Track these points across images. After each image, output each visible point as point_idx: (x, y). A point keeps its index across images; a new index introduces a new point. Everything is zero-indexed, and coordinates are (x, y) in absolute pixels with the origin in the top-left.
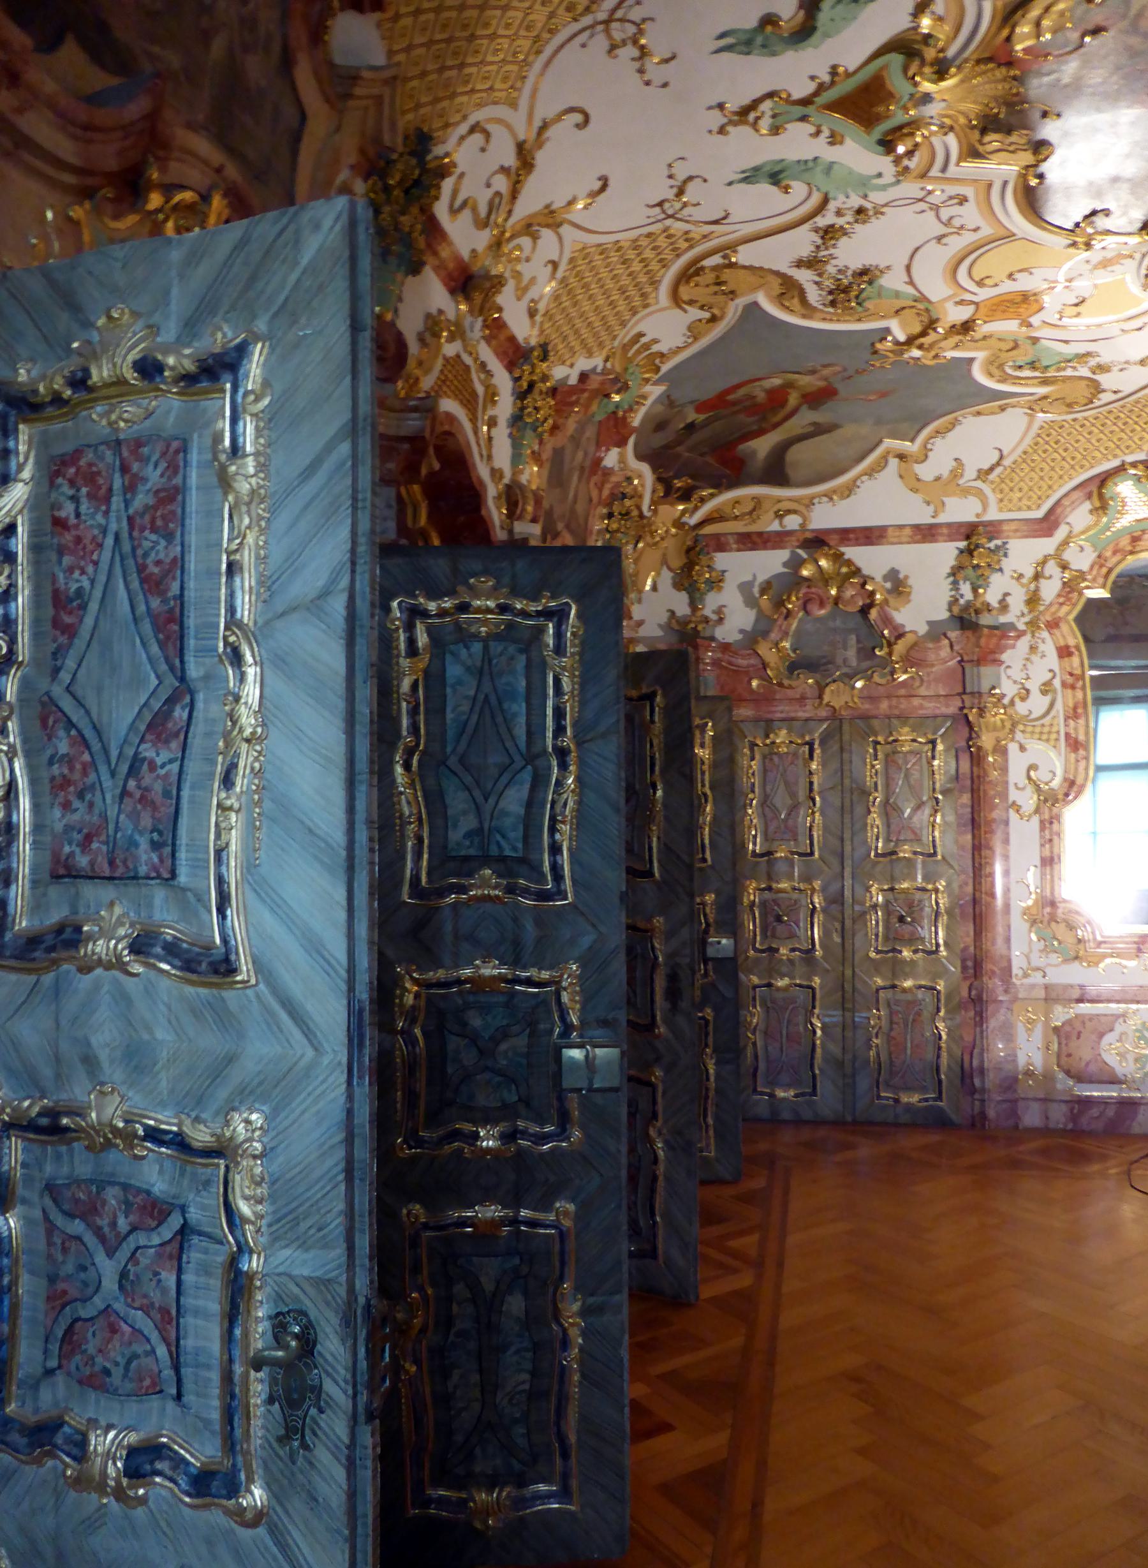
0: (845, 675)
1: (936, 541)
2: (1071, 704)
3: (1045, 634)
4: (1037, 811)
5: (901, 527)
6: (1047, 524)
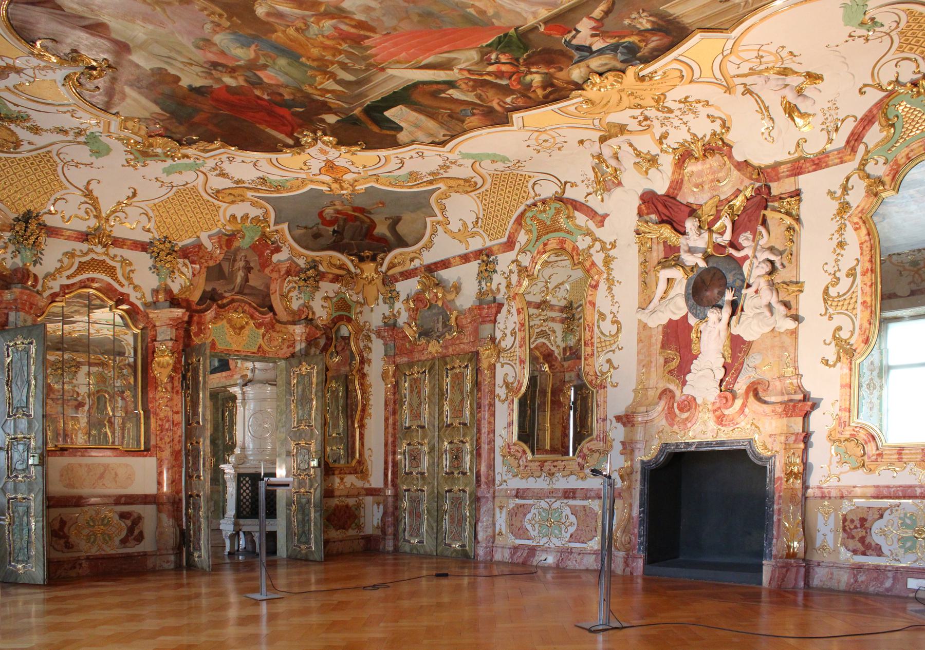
5: (454, 257)
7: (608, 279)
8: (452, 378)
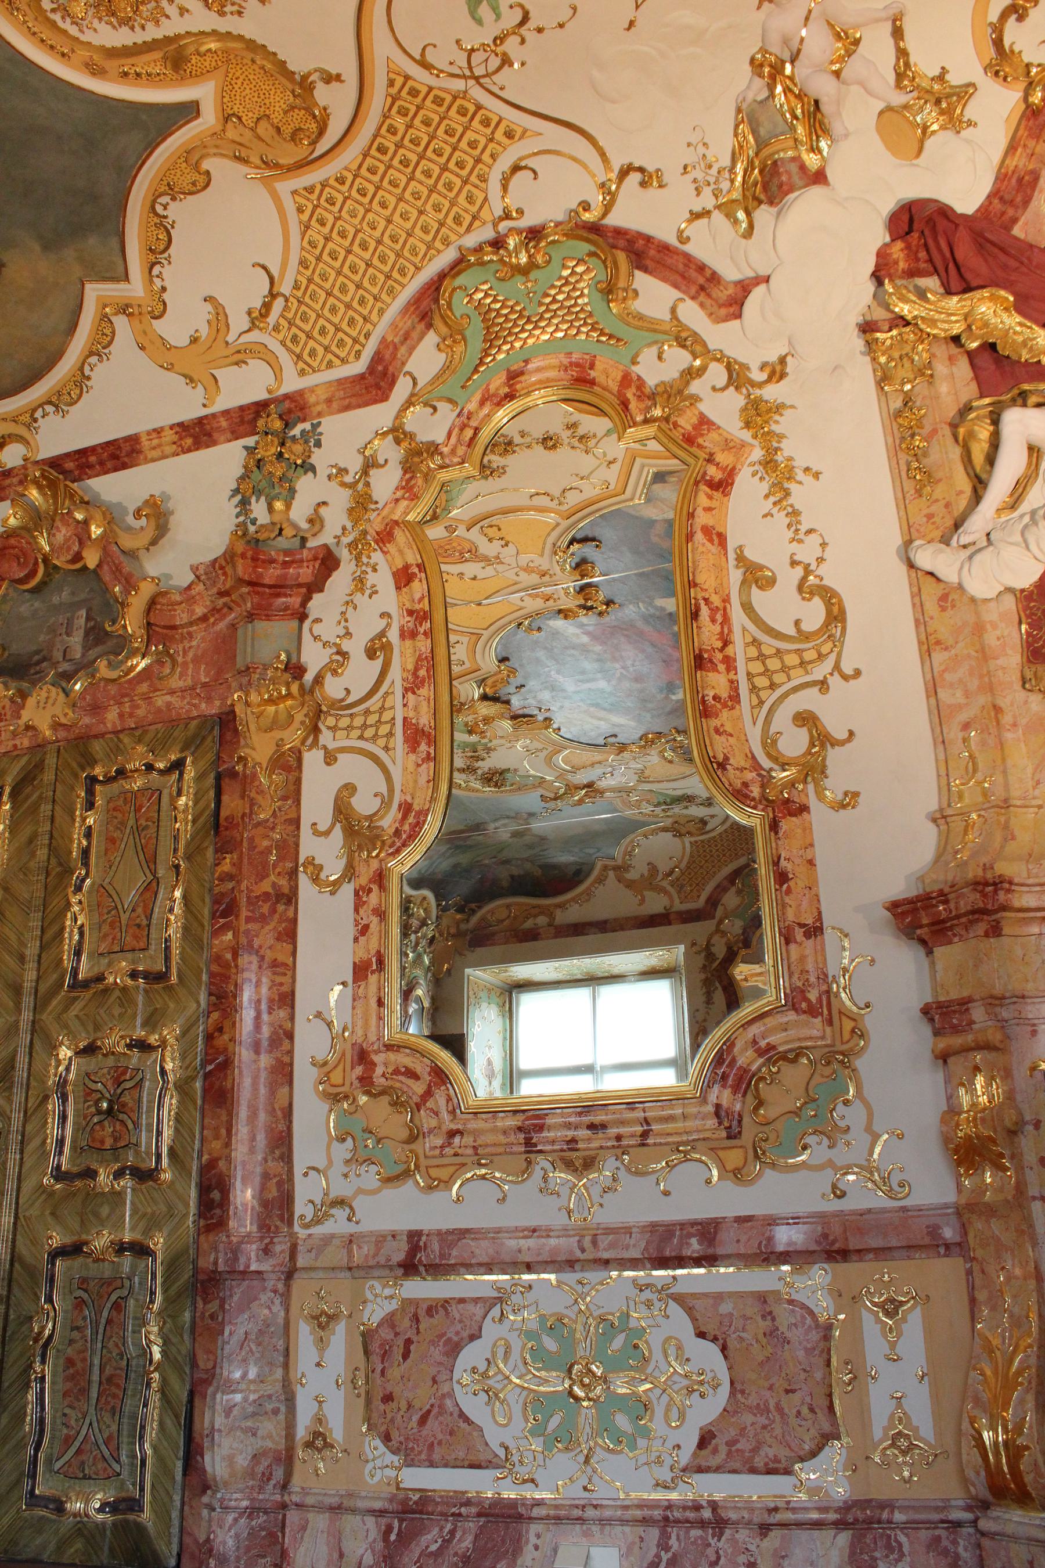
1: (214, 443)
2: (410, 667)
4: (350, 872)
5: (158, 431)
7: (769, 463)
8: (112, 809)
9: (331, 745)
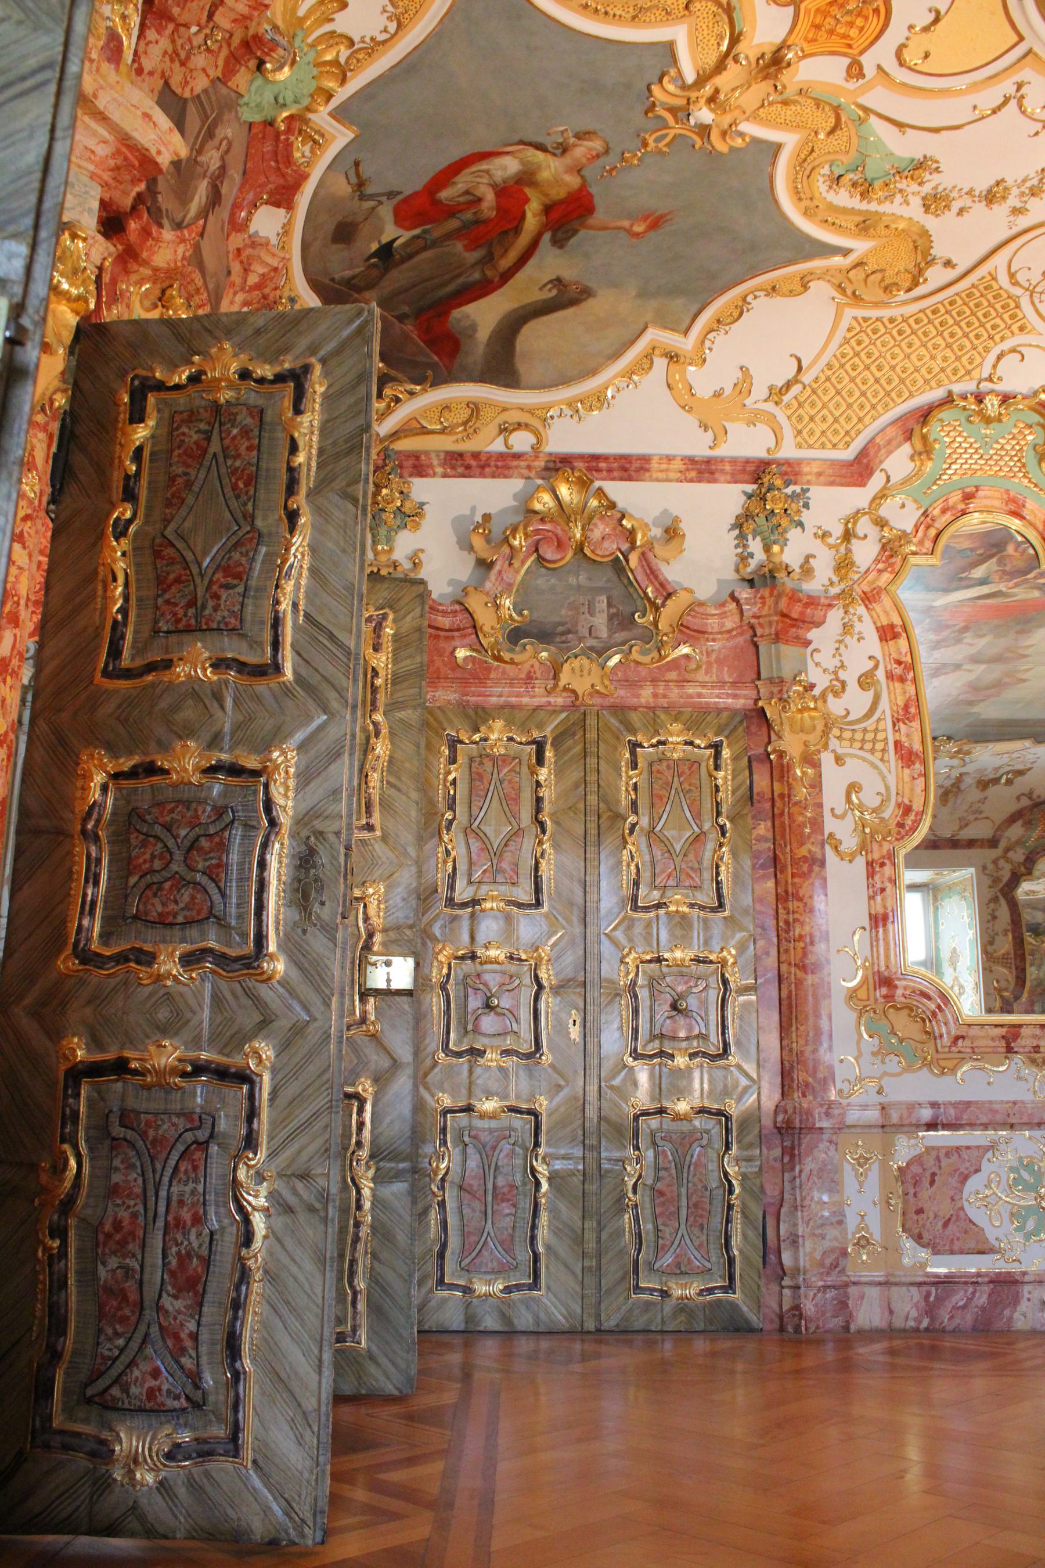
0: (592, 649)
1: (715, 481)
2: (901, 702)
3: (861, 610)
5: (669, 459)
6: (859, 470)
9: (840, 751)
